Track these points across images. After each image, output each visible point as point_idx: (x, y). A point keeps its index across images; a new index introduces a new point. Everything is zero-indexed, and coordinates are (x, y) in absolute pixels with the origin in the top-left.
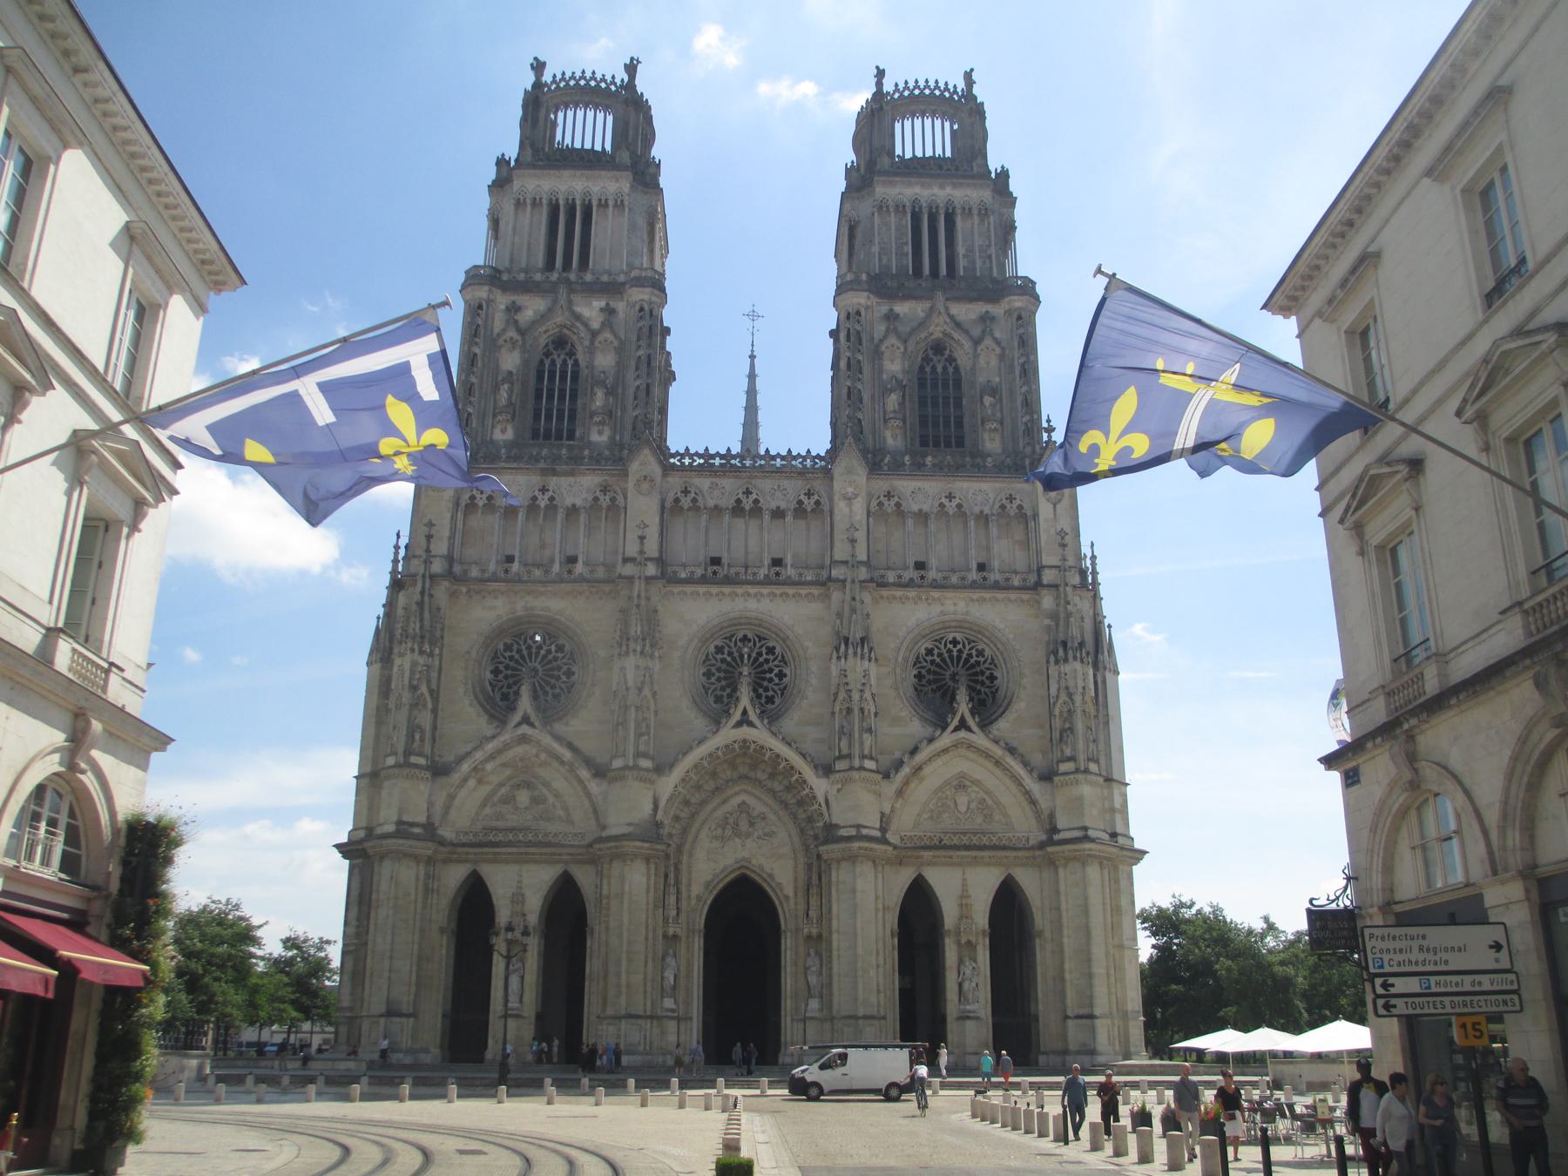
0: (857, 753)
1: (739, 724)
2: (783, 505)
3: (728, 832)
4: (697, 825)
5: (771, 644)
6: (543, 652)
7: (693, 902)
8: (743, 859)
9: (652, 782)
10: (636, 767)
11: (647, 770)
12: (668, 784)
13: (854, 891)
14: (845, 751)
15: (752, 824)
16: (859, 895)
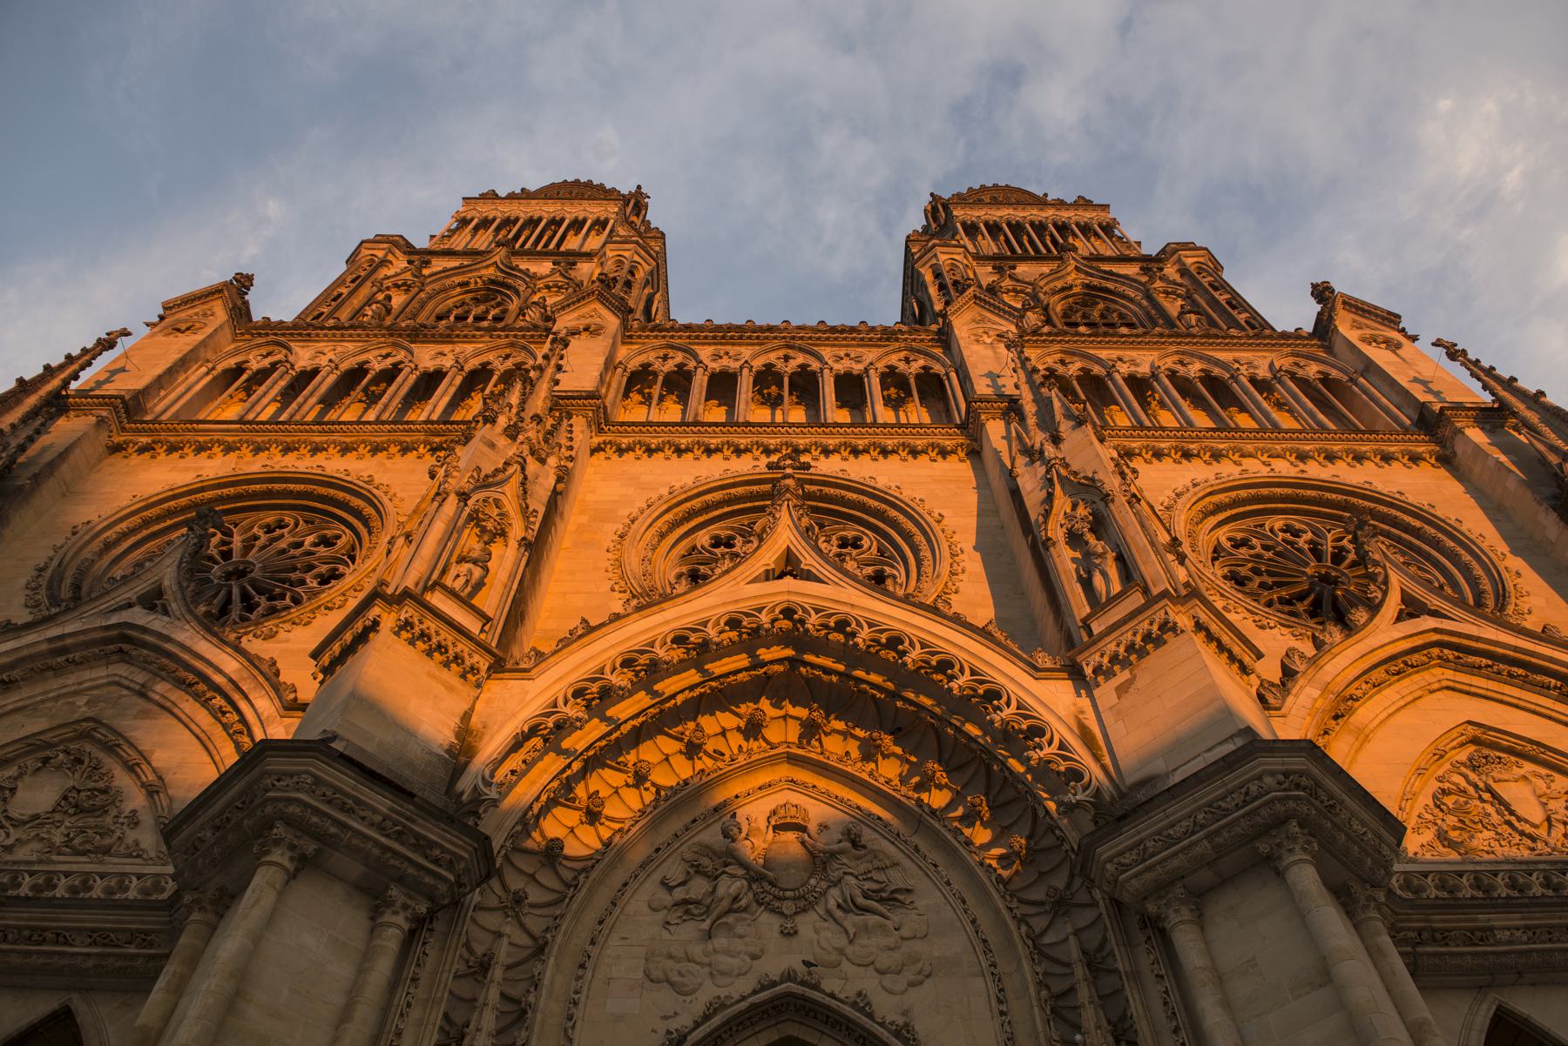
2: (858, 368)
5: (850, 534)
6: (283, 544)
8: (789, 976)
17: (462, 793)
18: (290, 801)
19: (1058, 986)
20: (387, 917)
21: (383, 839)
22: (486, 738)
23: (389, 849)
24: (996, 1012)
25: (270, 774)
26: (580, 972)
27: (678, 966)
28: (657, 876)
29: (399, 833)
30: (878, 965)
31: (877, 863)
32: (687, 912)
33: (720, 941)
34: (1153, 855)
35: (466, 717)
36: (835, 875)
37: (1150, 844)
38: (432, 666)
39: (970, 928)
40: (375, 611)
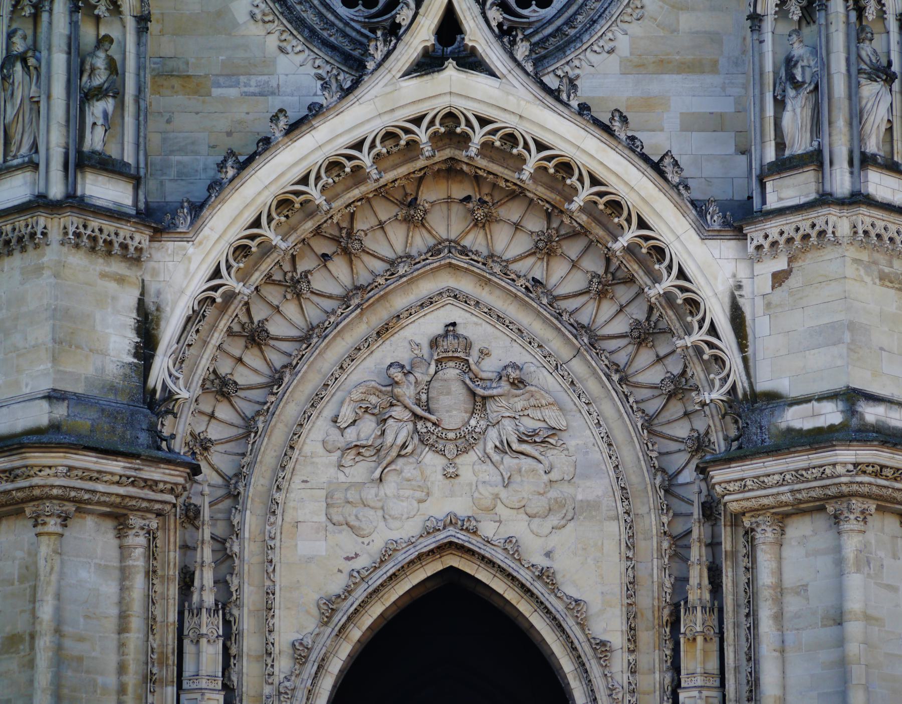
0: (840, 145)
1: (429, 63)
3: (399, 431)
4: (290, 411)
7: (283, 665)
8: (452, 521)
9: (136, 258)
10: (74, 202)
11: (114, 214)
12: (184, 269)
13: (838, 619)
14: (800, 144)
15: (479, 402)
16: (854, 628)
17: (154, 390)
18: (53, 486)
19: (679, 528)
20: (131, 540)
21: (121, 490)
22: (163, 324)
23: (123, 497)
24: (624, 556)
25: (32, 467)
26: (272, 519)
27: (354, 511)
28: (328, 412)
29: (133, 482)
30: (529, 510)
31: (533, 402)
32: (359, 454)
33: (390, 486)
34: (750, 490)
35: (141, 306)
36: (493, 417)
37: (749, 483)
38: (100, 265)
39: (612, 473)
40: (42, 220)
